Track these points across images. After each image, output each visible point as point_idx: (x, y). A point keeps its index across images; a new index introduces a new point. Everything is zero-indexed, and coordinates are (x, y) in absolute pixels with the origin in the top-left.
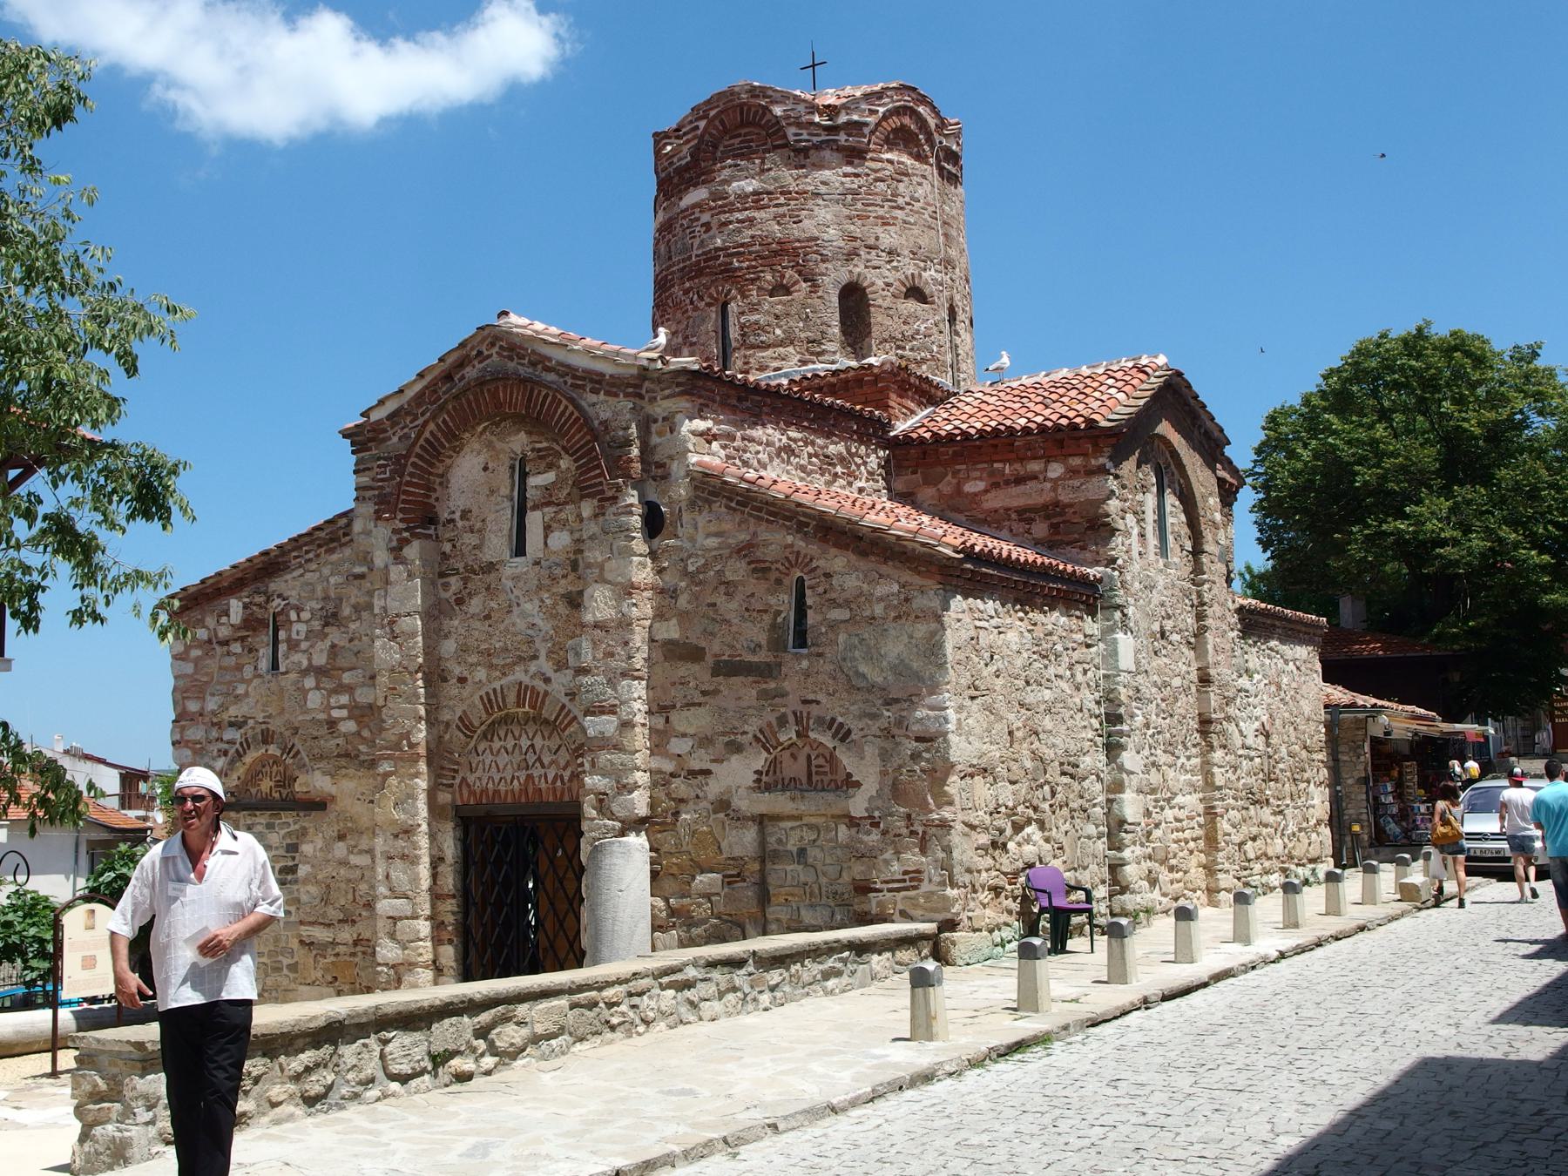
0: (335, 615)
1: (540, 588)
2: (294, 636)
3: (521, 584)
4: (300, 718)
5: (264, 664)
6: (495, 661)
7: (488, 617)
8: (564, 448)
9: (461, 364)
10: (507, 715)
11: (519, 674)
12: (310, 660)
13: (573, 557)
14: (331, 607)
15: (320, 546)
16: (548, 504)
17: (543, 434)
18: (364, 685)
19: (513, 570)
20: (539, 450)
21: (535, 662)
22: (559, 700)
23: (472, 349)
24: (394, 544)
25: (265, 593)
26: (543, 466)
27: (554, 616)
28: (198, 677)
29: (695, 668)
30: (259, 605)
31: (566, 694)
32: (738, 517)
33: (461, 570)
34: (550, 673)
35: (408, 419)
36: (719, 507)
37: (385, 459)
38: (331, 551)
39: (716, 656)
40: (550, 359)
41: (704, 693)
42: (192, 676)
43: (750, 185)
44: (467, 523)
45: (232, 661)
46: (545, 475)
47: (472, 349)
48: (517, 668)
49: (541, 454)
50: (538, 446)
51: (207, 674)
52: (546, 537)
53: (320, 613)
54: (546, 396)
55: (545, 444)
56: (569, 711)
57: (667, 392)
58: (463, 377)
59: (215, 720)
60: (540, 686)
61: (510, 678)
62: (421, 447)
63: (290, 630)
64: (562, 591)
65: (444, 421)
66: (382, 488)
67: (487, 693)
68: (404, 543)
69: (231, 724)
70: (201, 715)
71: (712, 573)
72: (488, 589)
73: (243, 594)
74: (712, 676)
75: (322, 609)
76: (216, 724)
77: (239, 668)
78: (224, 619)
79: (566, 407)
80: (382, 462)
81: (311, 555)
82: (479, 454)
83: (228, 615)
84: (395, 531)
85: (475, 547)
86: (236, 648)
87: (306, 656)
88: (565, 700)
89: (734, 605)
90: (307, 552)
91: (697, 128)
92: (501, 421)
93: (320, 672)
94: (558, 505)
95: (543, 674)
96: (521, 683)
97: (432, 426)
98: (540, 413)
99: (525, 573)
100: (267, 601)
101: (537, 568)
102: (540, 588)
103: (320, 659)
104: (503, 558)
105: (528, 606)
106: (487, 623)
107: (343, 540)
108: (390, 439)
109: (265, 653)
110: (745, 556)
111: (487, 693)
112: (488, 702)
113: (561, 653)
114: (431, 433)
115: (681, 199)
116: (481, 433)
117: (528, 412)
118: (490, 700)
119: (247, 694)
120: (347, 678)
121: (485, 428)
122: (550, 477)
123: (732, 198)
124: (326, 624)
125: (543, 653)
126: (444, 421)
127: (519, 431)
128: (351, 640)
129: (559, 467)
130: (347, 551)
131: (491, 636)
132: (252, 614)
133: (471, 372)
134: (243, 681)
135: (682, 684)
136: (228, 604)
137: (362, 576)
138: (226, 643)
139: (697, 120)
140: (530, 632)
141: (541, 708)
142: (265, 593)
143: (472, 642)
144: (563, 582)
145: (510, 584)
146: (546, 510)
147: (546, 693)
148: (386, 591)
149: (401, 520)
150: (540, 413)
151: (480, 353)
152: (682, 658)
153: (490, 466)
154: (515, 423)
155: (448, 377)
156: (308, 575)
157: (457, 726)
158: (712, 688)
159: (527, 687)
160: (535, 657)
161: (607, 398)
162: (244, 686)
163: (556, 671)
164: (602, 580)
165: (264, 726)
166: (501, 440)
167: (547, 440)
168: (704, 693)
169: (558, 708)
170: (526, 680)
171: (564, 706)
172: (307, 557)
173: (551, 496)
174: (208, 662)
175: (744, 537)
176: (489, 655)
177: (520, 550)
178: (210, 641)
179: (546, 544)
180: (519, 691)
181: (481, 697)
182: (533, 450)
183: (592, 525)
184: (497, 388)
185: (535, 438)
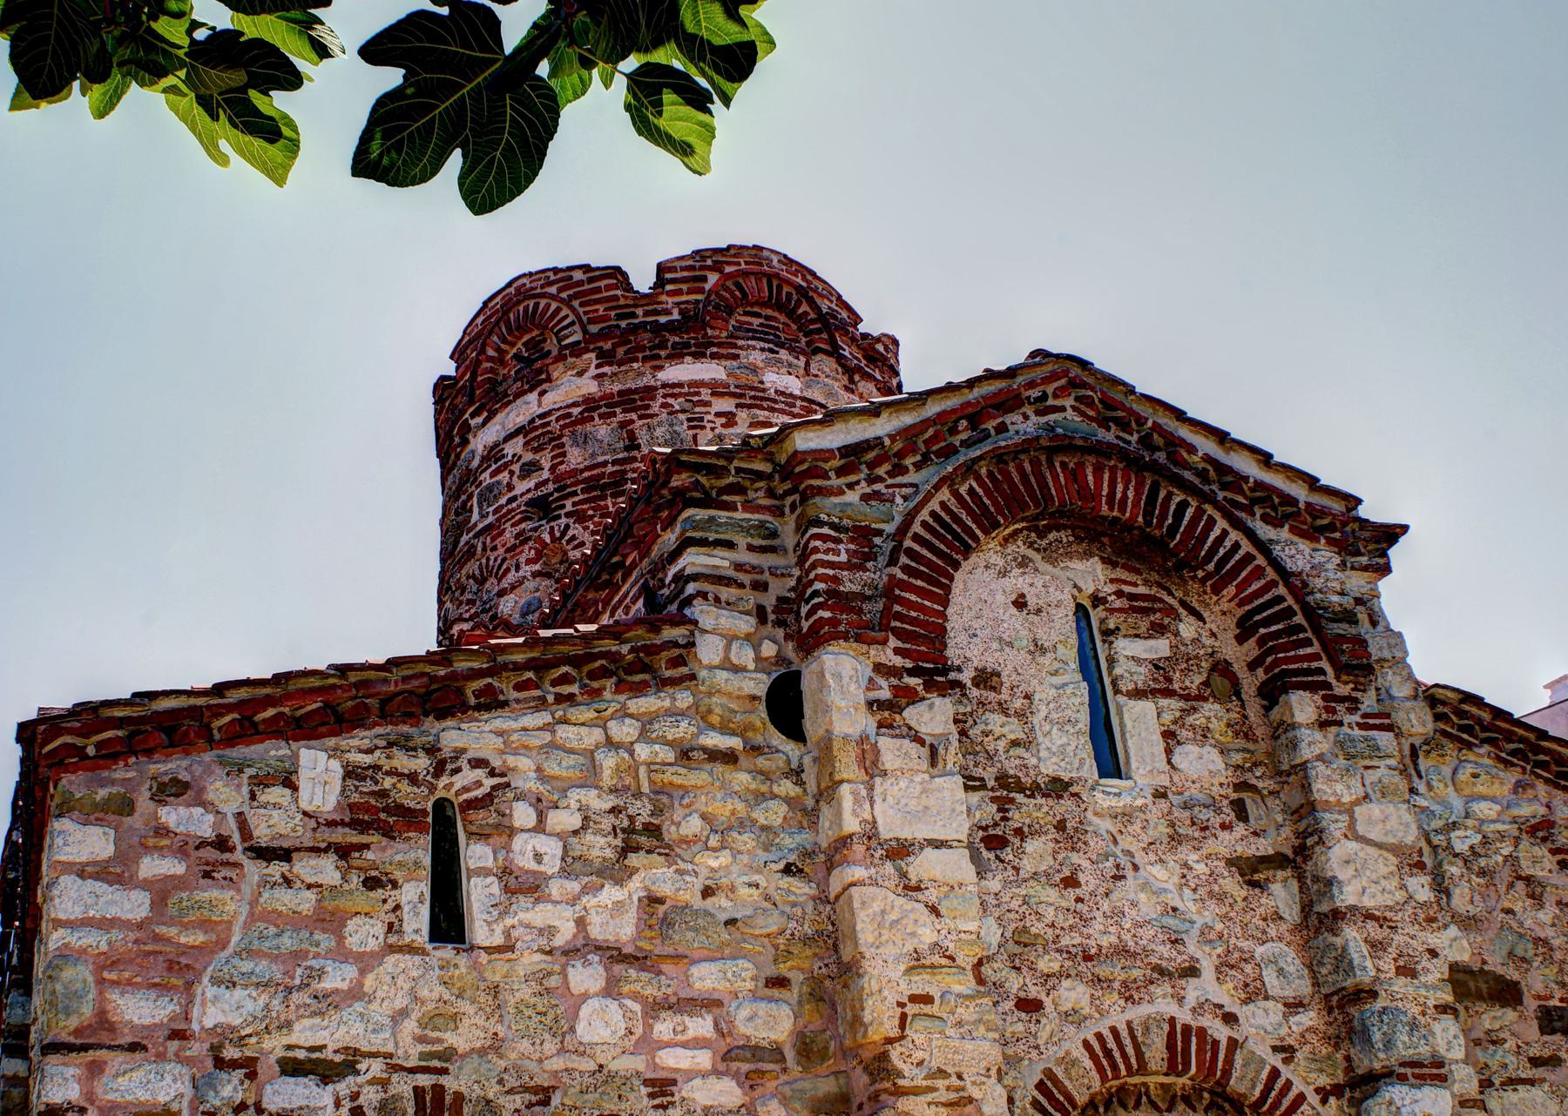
0: (653, 831)
1: (1176, 839)
2: (526, 862)
3: (1136, 827)
4: (557, 1064)
5: (417, 923)
6: (1103, 970)
7: (1071, 882)
8: (1183, 604)
9: (1008, 402)
10: (1122, 1088)
11: (1168, 1008)
12: (581, 923)
13: (1234, 796)
14: (642, 811)
15: (603, 673)
16: (1168, 693)
17: (1138, 572)
18: (755, 996)
19: (1113, 802)
20: (1132, 597)
21: (1193, 981)
22: (1263, 1062)
23: (1031, 385)
24: (885, 694)
25: (432, 750)
26: (1144, 625)
27: (1220, 898)
28: (161, 930)
29: (1510, 1015)
30: (413, 778)
31: (1275, 1049)
32: (1512, 776)
33: (991, 783)
34: (1232, 1007)
35: (886, 467)
36: (1482, 756)
37: (833, 526)
38: (639, 690)
39: (1539, 997)
40: (1192, 449)
41: (1536, 1062)
42: (140, 926)
43: (794, 385)
44: (992, 695)
45: (306, 902)
46: (1151, 642)
47: (1031, 385)
48: (1157, 990)
49: (1138, 606)
50: (1127, 589)
51: (205, 925)
52: (1169, 752)
53: (607, 822)
54: (1183, 506)
55: (1142, 590)
56: (1288, 1084)
57: (1364, 560)
58: (1001, 428)
59: (230, 1053)
60: (1221, 1032)
61: (1144, 1010)
62: (924, 524)
63: (508, 848)
64: (1225, 852)
65: (971, 491)
66: (835, 579)
67: (1099, 1036)
68: (901, 697)
69: (292, 1068)
70: (178, 1035)
71: (1500, 859)
72: (1061, 826)
73: (355, 742)
74: (1542, 1033)
75: (614, 810)
76: (234, 1064)
77: (330, 920)
78: (277, 794)
79: (1225, 533)
80: (826, 530)
81: (574, 689)
82: (1003, 573)
83: (290, 784)
84: (879, 668)
85: (1015, 743)
86: (326, 870)
87: (569, 912)
88: (1276, 1060)
89: (1546, 915)
90: (565, 679)
91: (705, 279)
92: (1049, 529)
93: (615, 955)
94: (1187, 698)
95: (1221, 1006)
96: (1172, 1021)
97: (945, 494)
98: (1174, 529)
99: (1145, 807)
100: (439, 769)
101: (1163, 804)
102: (1176, 839)
103: (624, 930)
104: (1084, 773)
105: (1157, 871)
106: (1071, 893)
107: (668, 674)
108: (841, 492)
109: (415, 895)
110: (1544, 840)
111: (1099, 1036)
112: (1102, 1053)
113: (1248, 968)
114: (943, 505)
115: (661, 368)
116: (1006, 540)
117: (1148, 523)
118: (1108, 1053)
119: (356, 993)
120: (706, 978)
121: (1016, 533)
122: (1160, 647)
123: (772, 391)
124: (627, 849)
125: (1207, 967)
126: (971, 491)
127: (1087, 555)
128: (707, 892)
129: (1177, 634)
130: (684, 699)
131: (1086, 921)
132: (383, 794)
133: (1023, 424)
134: (342, 954)
135: (1494, 1043)
136: (296, 756)
137: (729, 758)
138: (285, 855)
139: (703, 268)
140: (1170, 921)
141: (1227, 1073)
142: (432, 750)
143: (1037, 928)
144: (1224, 835)
145: (1105, 825)
146: (1164, 702)
147: (1233, 1044)
148: (871, 789)
149: (897, 651)
150: (1174, 529)
151: (1044, 397)
152: (1481, 998)
153: (1032, 601)
154: (1079, 540)
155: (975, 416)
156: (565, 733)
157: (1036, 1104)
158: (1547, 1053)
159: (1187, 1029)
160: (1192, 971)
161: (1295, 539)
162: (351, 971)
163: (1246, 1002)
164: (1352, 834)
165: (425, 1080)
166: (1052, 561)
167: (1146, 582)
168: (1536, 1062)
169: (1264, 1075)
170: (1184, 1016)
171: (1275, 1073)
172: (566, 689)
173: (1169, 680)
174: (210, 894)
175: (1529, 810)
176: (1088, 958)
177: (1110, 763)
178: (222, 843)
179: (1169, 762)
180: (1171, 1035)
181: (1086, 1044)
182: (1119, 594)
183: (1318, 735)
184: (1081, 466)
185: (1120, 574)
